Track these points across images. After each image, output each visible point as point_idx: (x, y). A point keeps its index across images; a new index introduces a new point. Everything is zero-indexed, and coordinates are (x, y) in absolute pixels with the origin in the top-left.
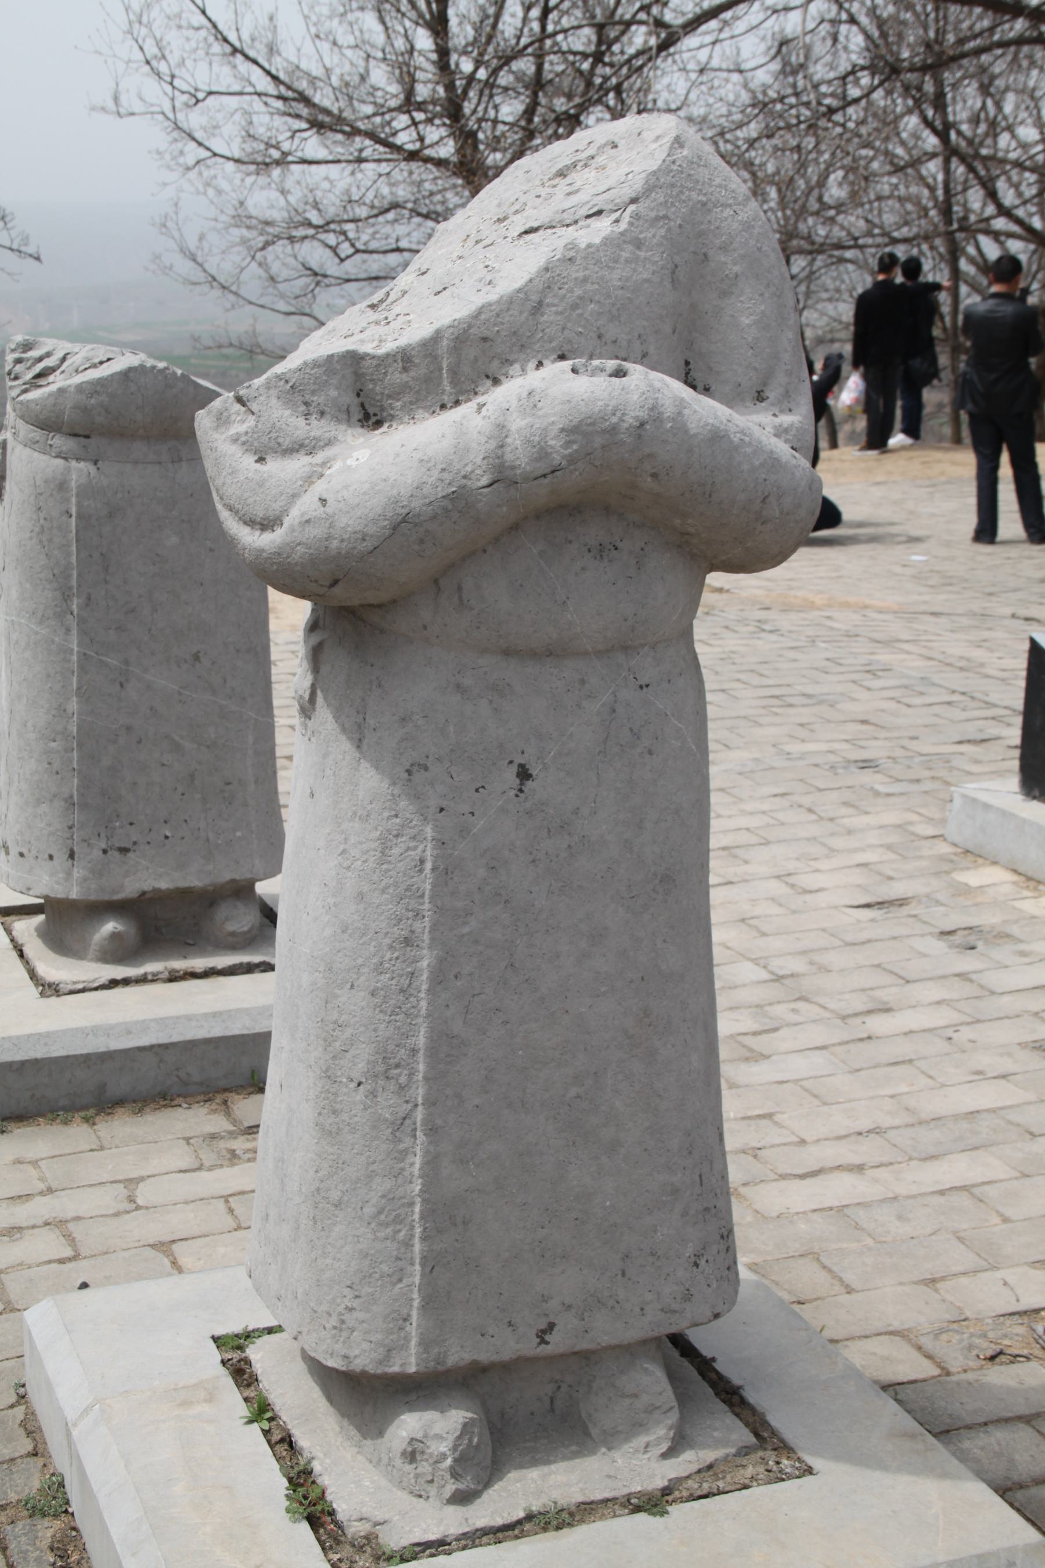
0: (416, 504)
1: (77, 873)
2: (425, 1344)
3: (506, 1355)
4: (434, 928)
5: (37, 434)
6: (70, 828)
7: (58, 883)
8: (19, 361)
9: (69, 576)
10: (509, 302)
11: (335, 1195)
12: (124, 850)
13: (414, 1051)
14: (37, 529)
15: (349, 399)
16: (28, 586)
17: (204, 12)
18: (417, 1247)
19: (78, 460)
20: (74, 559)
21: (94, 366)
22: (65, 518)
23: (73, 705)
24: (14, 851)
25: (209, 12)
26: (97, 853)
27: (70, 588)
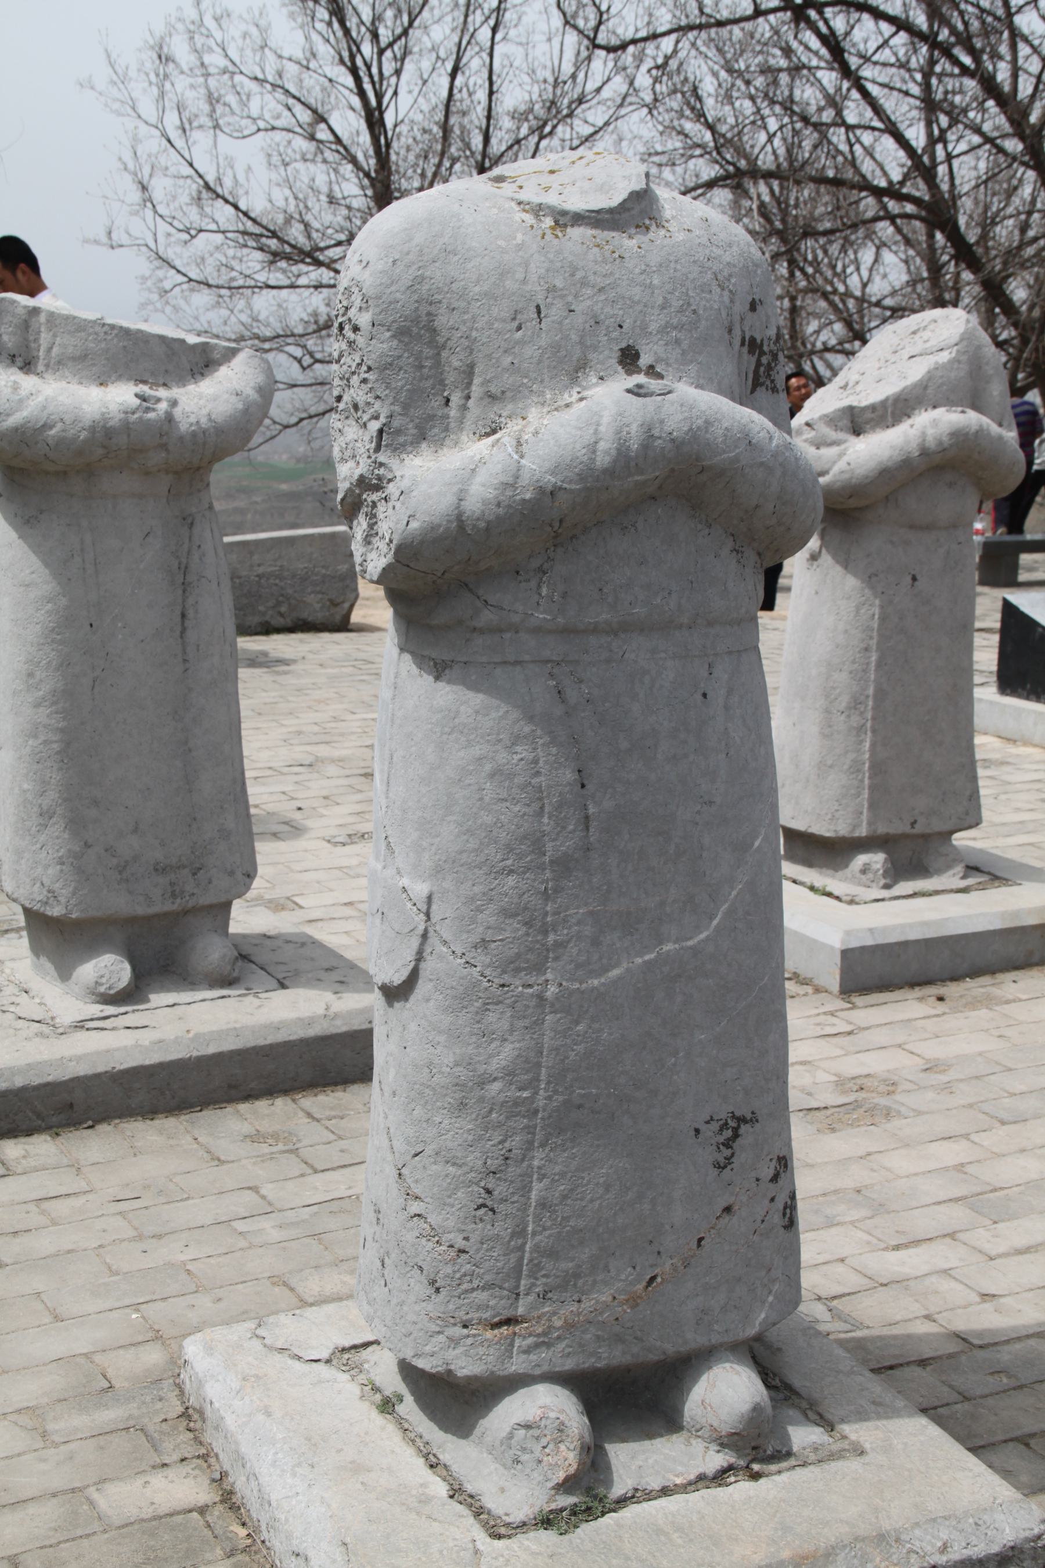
0: (890, 464)
2: (870, 824)
3: (900, 831)
4: (878, 643)
10: (915, 386)
11: (829, 762)
13: (867, 697)
15: (849, 425)
17: (191, 165)
18: (867, 781)
25: (195, 165)
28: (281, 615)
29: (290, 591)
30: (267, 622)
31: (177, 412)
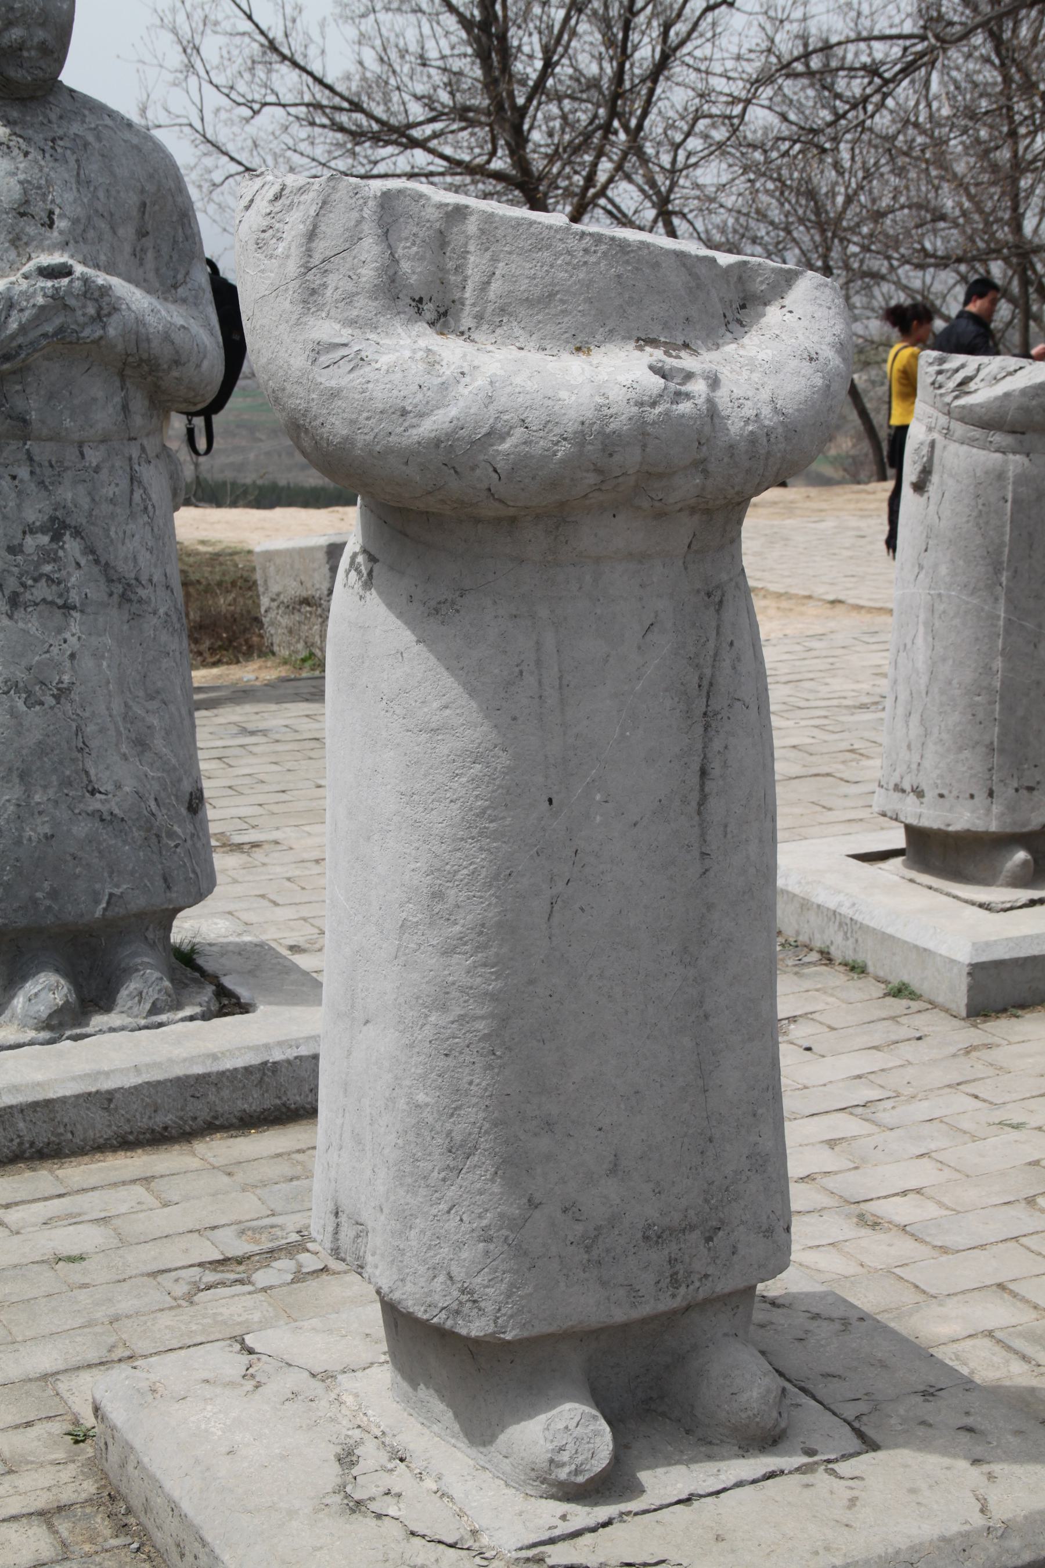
1: (996, 809)
5: (977, 433)
6: (990, 770)
7: (978, 818)
9: (1002, 553)
12: (1030, 789)
14: (974, 514)
16: (961, 563)
17: (250, 17)
19: (1014, 453)
20: (1007, 538)
21: (1010, 374)
22: (1001, 503)
23: (998, 664)
24: (930, 795)
25: (255, 17)
26: (1011, 791)
27: (1001, 563)
31: (722, 398)
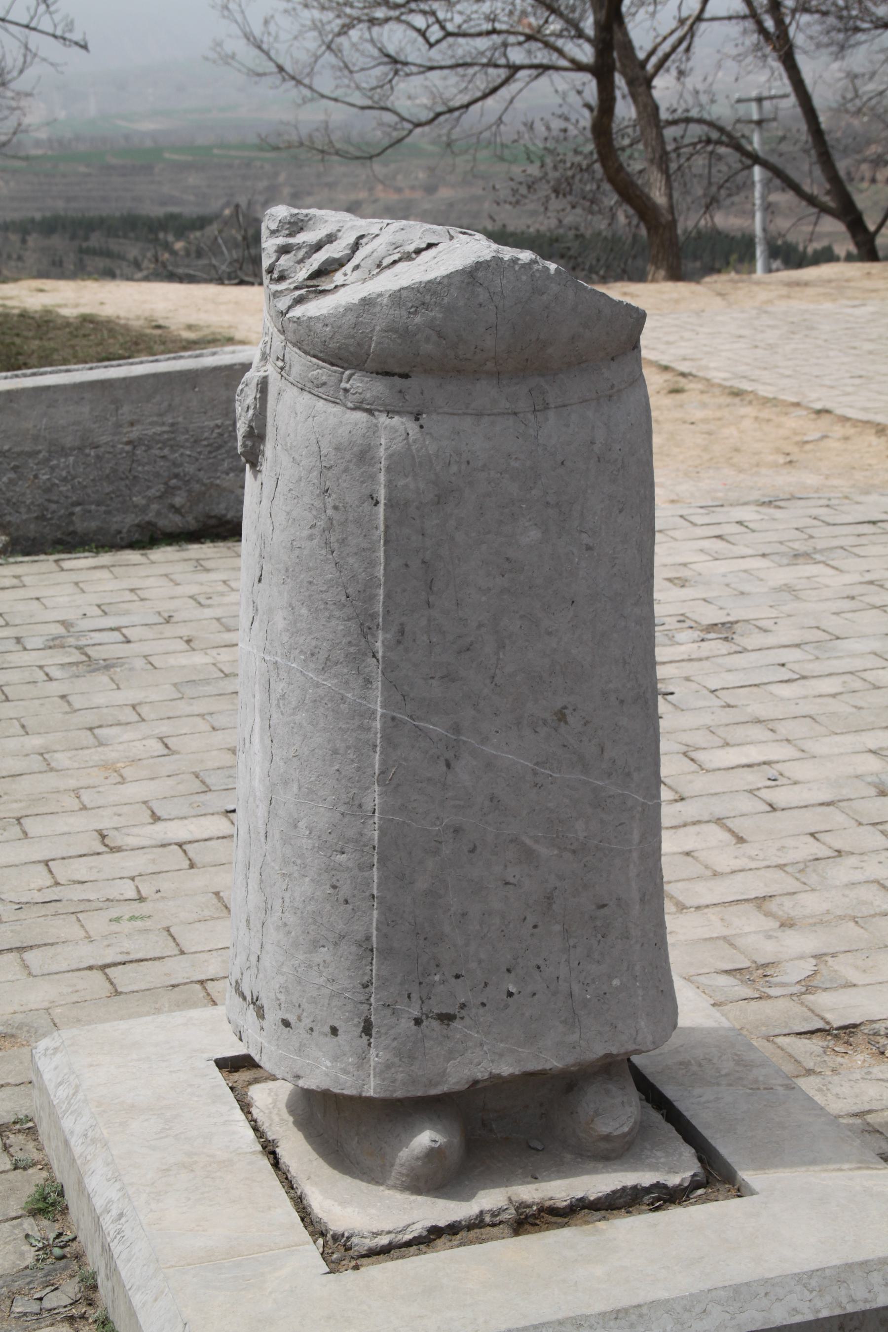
1: (376, 1057)
5: (324, 372)
6: (365, 986)
7: (345, 1071)
8: (284, 250)
9: (372, 598)
12: (446, 1018)
14: (321, 524)
16: (304, 611)
19: (389, 413)
20: (380, 571)
21: (407, 257)
22: (367, 506)
23: (374, 798)
26: (406, 1025)
27: (373, 616)
28: (177, 510)
29: (190, 469)
30: (149, 523)
